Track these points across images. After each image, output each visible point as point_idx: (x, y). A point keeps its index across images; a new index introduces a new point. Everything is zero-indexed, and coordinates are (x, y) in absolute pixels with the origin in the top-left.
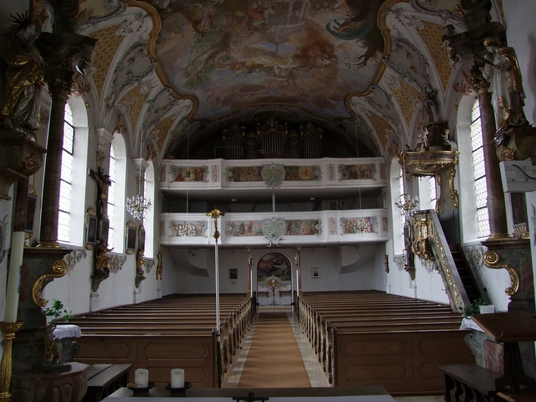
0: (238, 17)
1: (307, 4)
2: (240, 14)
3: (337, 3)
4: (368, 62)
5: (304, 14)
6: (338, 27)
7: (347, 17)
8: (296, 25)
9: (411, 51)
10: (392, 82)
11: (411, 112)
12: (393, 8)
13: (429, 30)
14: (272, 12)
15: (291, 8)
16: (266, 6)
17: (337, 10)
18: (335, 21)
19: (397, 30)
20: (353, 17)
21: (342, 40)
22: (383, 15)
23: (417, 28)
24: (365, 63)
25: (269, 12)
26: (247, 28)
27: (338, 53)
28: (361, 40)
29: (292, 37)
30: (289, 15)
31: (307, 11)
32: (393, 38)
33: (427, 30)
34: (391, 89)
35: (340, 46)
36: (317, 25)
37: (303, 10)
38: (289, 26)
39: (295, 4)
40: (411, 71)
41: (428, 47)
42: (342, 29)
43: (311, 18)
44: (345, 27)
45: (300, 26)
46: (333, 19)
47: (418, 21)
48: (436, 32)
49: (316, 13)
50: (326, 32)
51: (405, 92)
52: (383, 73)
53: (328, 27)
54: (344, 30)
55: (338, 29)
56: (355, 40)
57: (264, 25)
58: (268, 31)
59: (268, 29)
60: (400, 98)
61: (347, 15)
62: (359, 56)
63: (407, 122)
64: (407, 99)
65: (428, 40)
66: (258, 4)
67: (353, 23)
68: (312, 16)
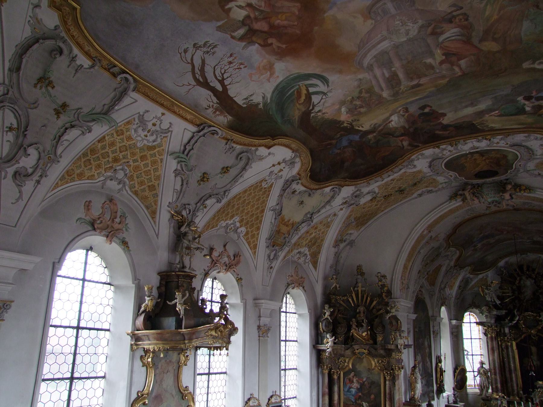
0: (494, 40)
1: (382, 90)
2: (491, 46)
3: (347, 113)
4: (205, 93)
5: (375, 77)
6: (311, 90)
7: (317, 109)
8: (374, 52)
9: (233, 172)
10: (150, 126)
11: (88, 174)
12: (298, 160)
13: (261, 193)
14: (429, 61)
15: (401, 75)
16: (444, 66)
17: (337, 107)
18: (325, 94)
19: (266, 157)
20: (312, 115)
21: (281, 79)
22: (293, 146)
23: (264, 180)
24: (205, 84)
25: (434, 59)
26: (471, 19)
27: (254, 52)
28: (265, 104)
29: (363, 26)
30: (397, 65)
31: (374, 82)
32: (253, 148)
33: (261, 190)
34: (128, 123)
35: (270, 68)
36: (340, 72)
37: (381, 81)
38: (385, 45)
39: (399, 83)
40: (197, 175)
41: (240, 194)
42: (304, 92)
43: (360, 76)
44: (303, 97)
45: (365, 55)
46: (329, 94)
47: (273, 181)
48: (258, 200)
49: (359, 86)
50: (317, 71)
51: (133, 154)
52: (174, 113)
53: (325, 81)
54: (299, 93)
55: (307, 87)
56: (269, 96)
57: (435, 34)
58: (420, 22)
59: (422, 27)
60: (112, 144)
61: (319, 111)
62: (226, 82)
63: (62, 178)
64: (116, 160)
65: (248, 192)
66: (459, 66)
67: (303, 110)
68: (360, 79)
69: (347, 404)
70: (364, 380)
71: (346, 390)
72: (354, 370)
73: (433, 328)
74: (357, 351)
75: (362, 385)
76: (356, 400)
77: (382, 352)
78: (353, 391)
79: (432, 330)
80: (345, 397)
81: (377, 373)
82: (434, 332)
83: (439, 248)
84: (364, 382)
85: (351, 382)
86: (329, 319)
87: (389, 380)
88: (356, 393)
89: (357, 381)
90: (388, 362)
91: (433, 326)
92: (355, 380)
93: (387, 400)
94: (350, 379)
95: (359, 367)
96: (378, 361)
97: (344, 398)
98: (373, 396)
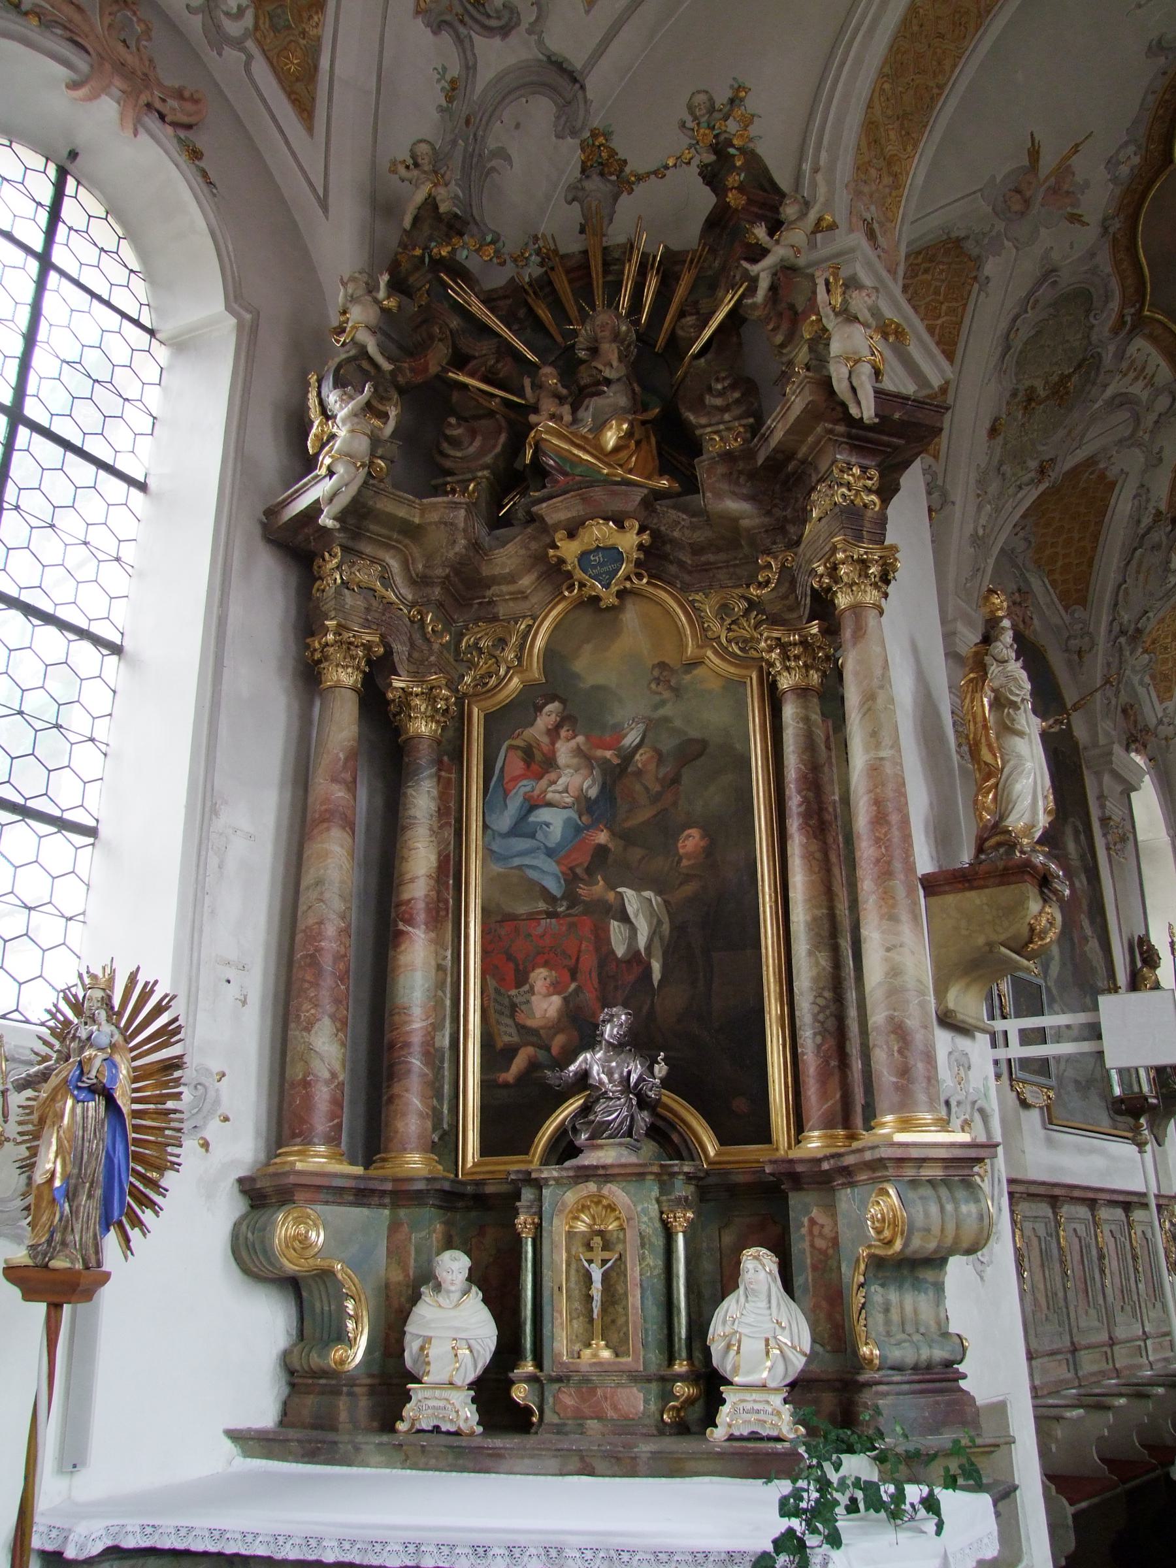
69: (511, 918)
70: (631, 738)
71: (504, 821)
72: (556, 684)
73: (1102, 807)
74: (569, 550)
75: (616, 775)
76: (571, 879)
77: (735, 506)
78: (554, 822)
79: (1095, 813)
80: (497, 868)
81: (715, 685)
82: (1105, 821)
83: (1081, 300)
84: (628, 757)
85: (540, 763)
86: (372, 349)
87: (802, 692)
88: (576, 830)
89: (578, 752)
90: (788, 576)
91: (1101, 797)
92: (564, 752)
93: (794, 824)
94: (528, 753)
95: (593, 667)
96: (724, 609)
97: (489, 881)
98: (691, 841)
